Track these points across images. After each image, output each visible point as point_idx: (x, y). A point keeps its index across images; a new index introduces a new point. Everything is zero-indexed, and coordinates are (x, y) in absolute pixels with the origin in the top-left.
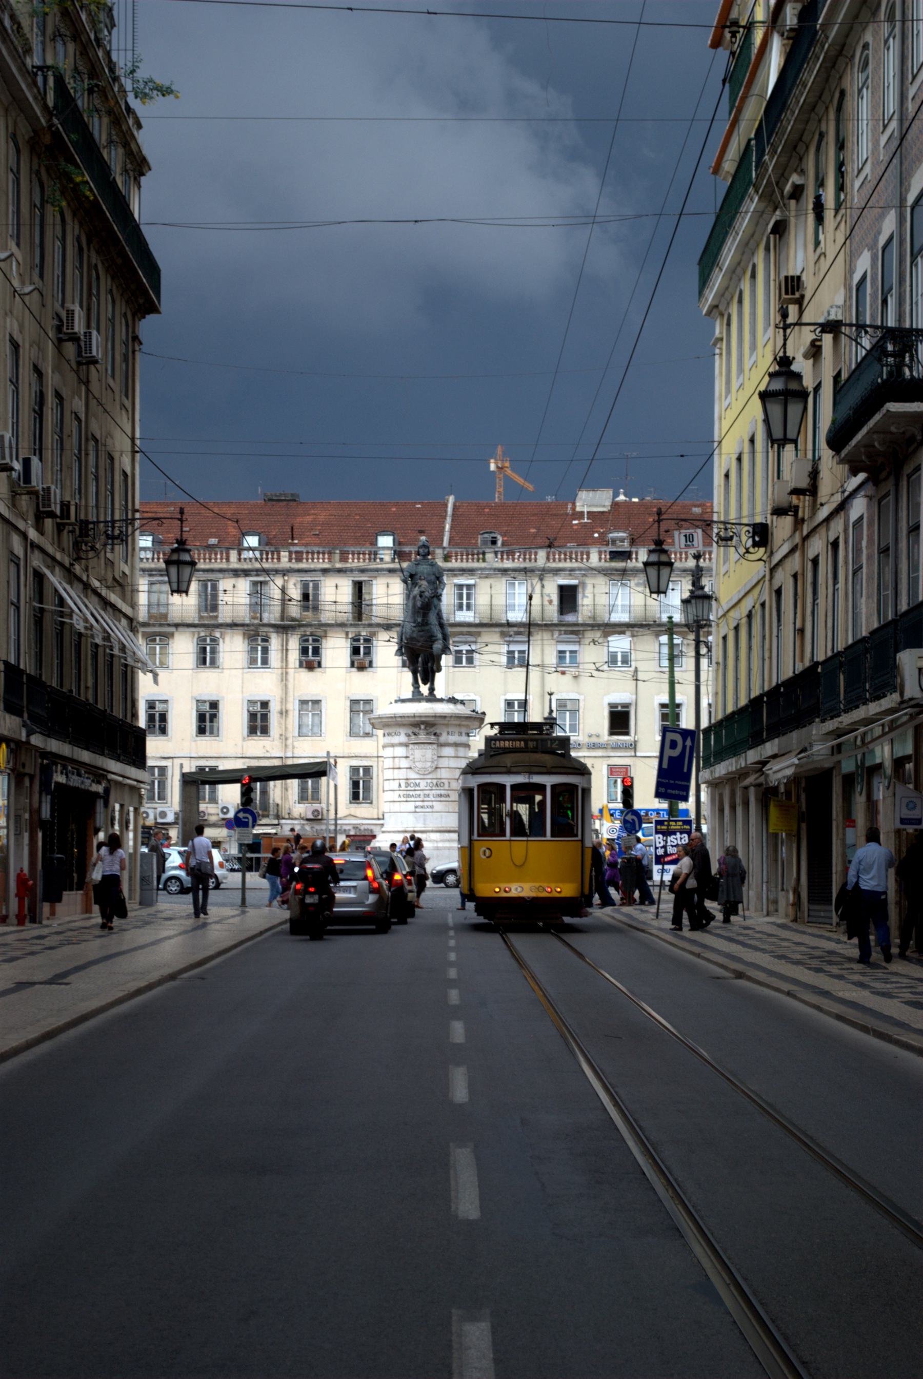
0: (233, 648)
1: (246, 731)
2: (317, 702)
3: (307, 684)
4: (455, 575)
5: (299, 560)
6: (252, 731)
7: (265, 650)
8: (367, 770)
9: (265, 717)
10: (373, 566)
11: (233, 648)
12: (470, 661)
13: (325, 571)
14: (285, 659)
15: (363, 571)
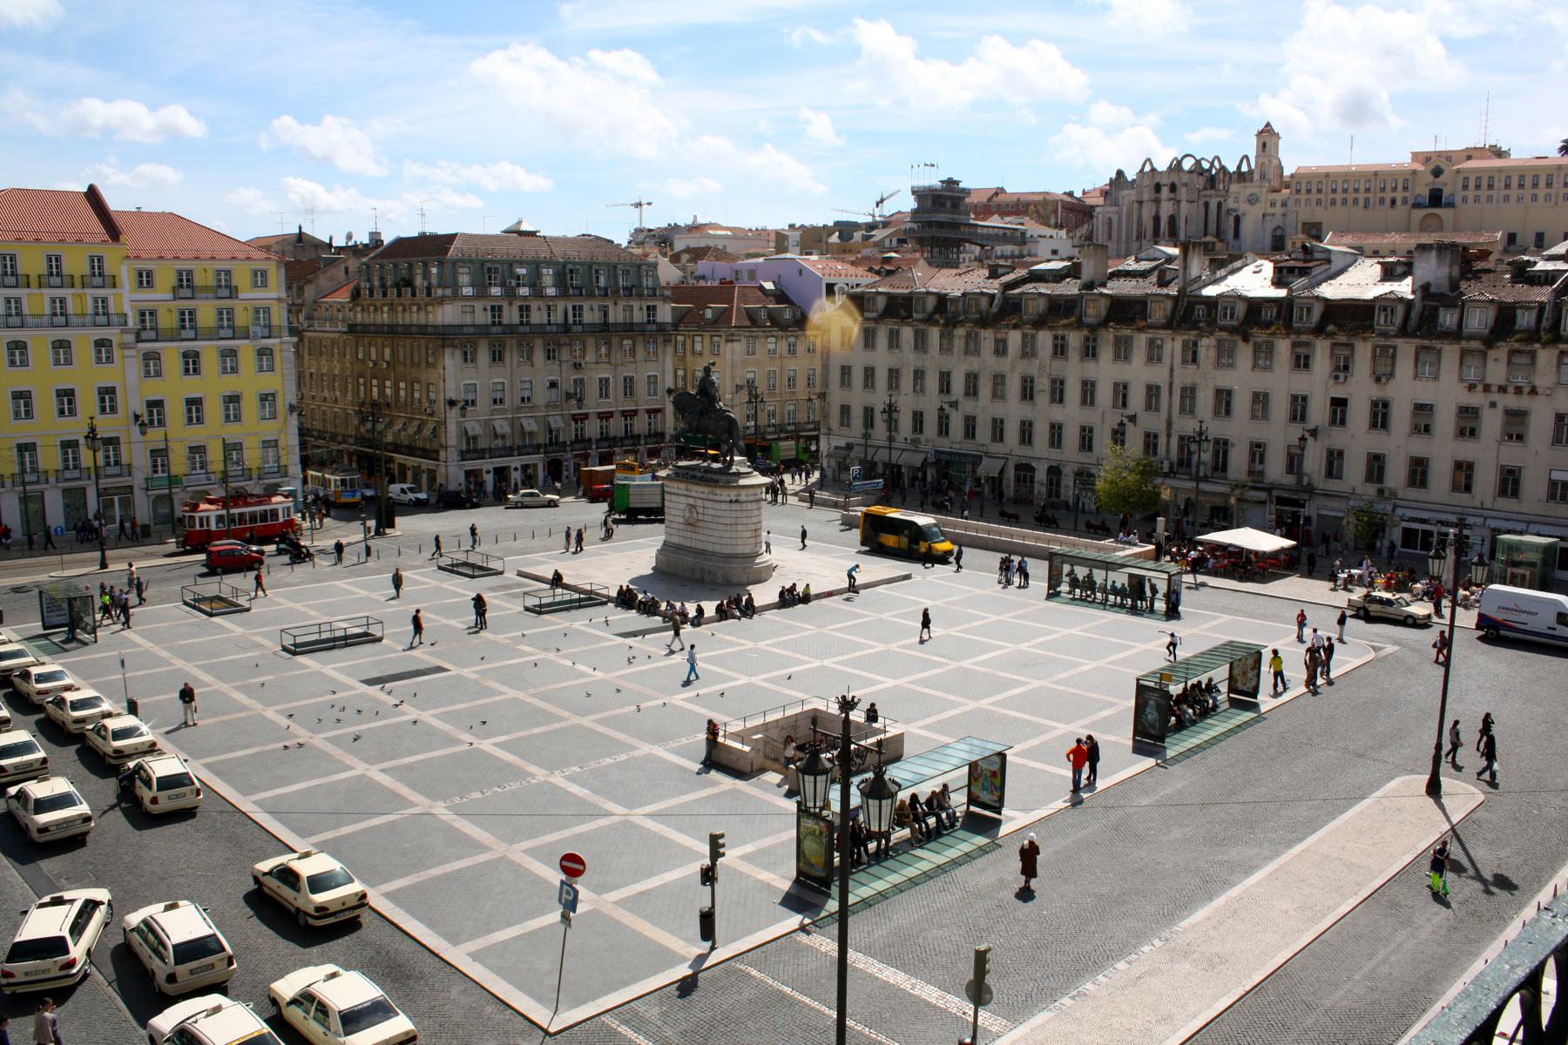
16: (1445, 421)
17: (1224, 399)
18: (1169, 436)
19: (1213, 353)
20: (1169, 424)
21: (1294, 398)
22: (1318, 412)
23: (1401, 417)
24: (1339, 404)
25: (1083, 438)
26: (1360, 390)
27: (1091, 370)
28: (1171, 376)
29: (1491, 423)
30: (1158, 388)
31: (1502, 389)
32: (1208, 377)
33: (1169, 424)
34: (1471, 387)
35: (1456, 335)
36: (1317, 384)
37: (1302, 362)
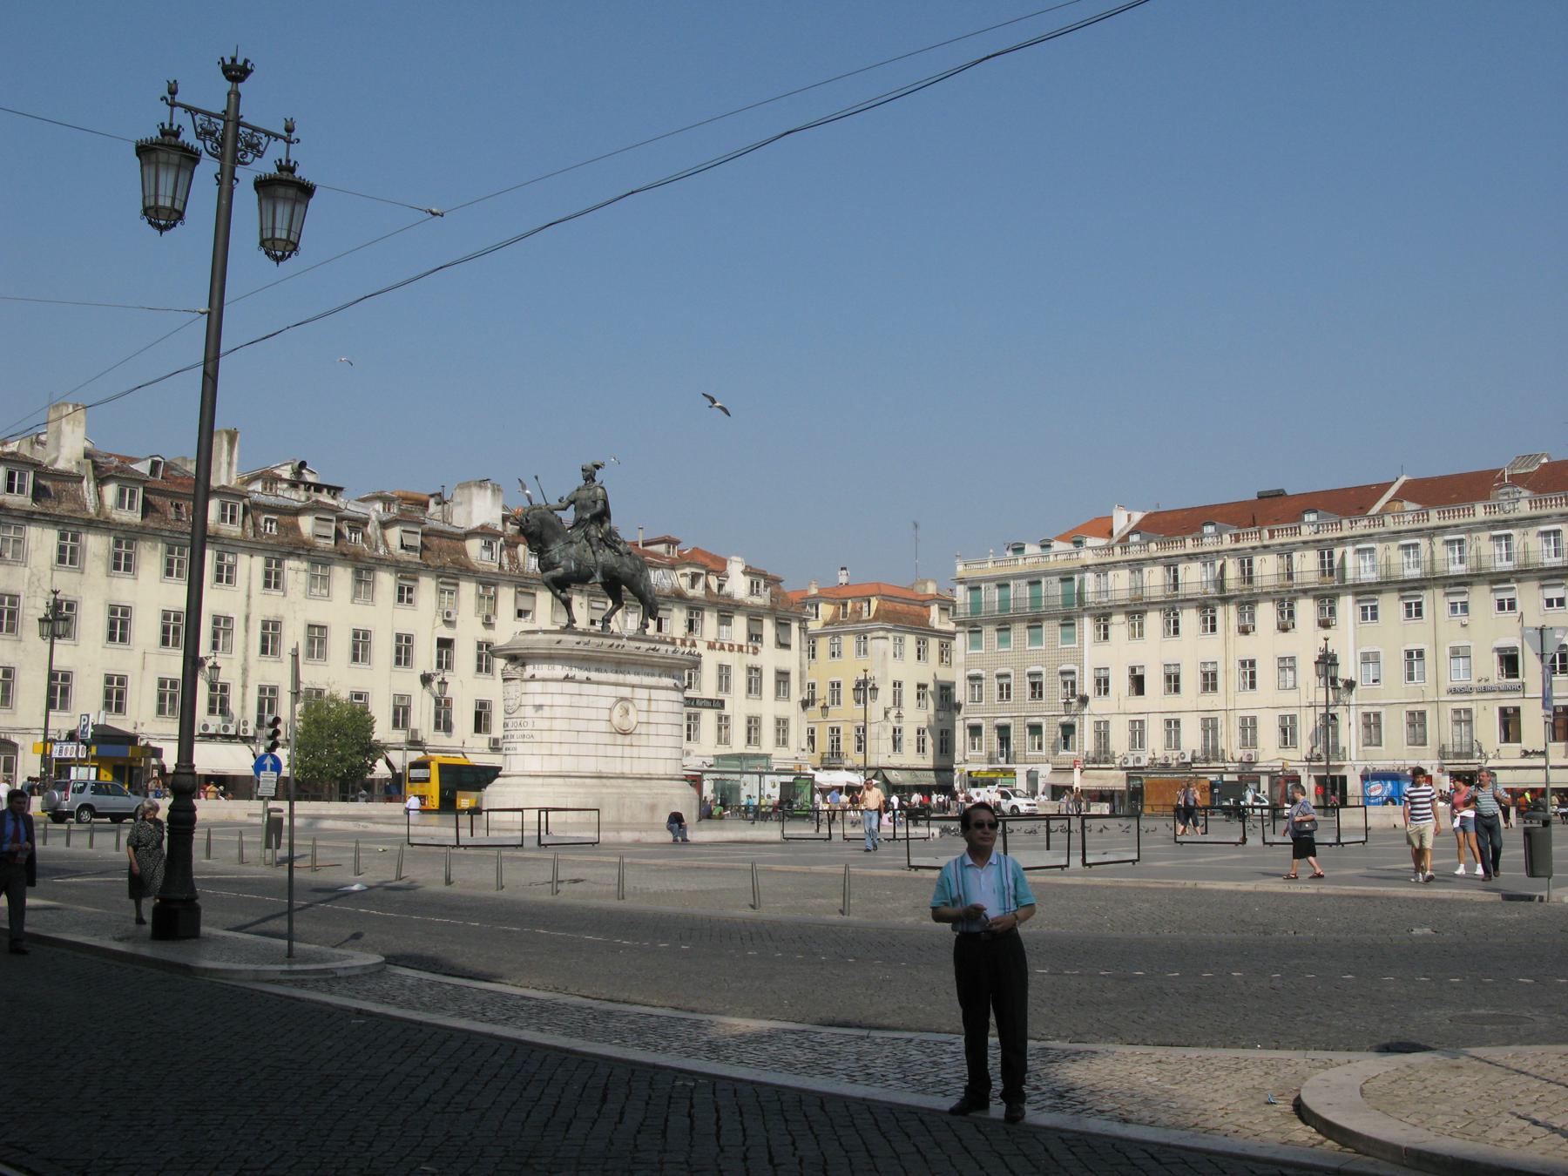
0: (1190, 619)
1: (1200, 688)
2: (1292, 659)
3: (1246, 647)
4: (1358, 542)
5: (1237, 540)
6: (1205, 688)
7: (1213, 619)
8: (1293, 718)
9: (1214, 675)
10: (1293, 539)
11: (1190, 619)
12: (1374, 617)
13: (1253, 548)
14: (1226, 627)
15: (1282, 545)
17: (317, 635)
18: (244, 686)
19: (303, 577)
20: (245, 671)
21: (399, 637)
22: (425, 656)
24: (445, 644)
25: (108, 694)
27: (124, 589)
28: (248, 605)
30: (228, 620)
33: (245, 671)
37: (404, 595)
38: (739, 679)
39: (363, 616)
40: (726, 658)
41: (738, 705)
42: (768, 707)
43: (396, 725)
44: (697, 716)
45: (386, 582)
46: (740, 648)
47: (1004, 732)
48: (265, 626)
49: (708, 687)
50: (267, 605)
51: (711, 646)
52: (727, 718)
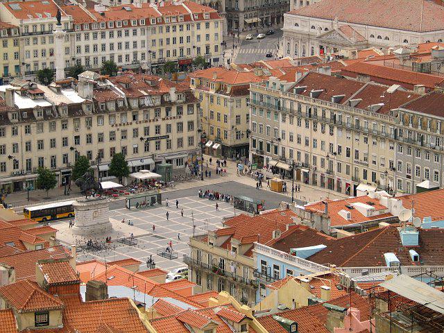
16: (107, 137)
19: (35, 129)
20: (22, 157)
22: (71, 142)
23: (95, 138)
24: (77, 138)
26: (83, 132)
29: (118, 135)
30: (17, 144)
31: (120, 125)
32: (34, 137)
33: (22, 157)
34: (113, 126)
35: (106, 111)
36: (70, 133)
37: (64, 127)
38: (174, 128)
39: (53, 135)
40: (169, 122)
41: (174, 136)
42: (186, 134)
43: (64, 163)
44: (159, 142)
45: (59, 124)
46: (174, 118)
47: (261, 143)
48: (26, 143)
49: (163, 132)
50: (26, 138)
51: (164, 119)
52: (170, 140)
